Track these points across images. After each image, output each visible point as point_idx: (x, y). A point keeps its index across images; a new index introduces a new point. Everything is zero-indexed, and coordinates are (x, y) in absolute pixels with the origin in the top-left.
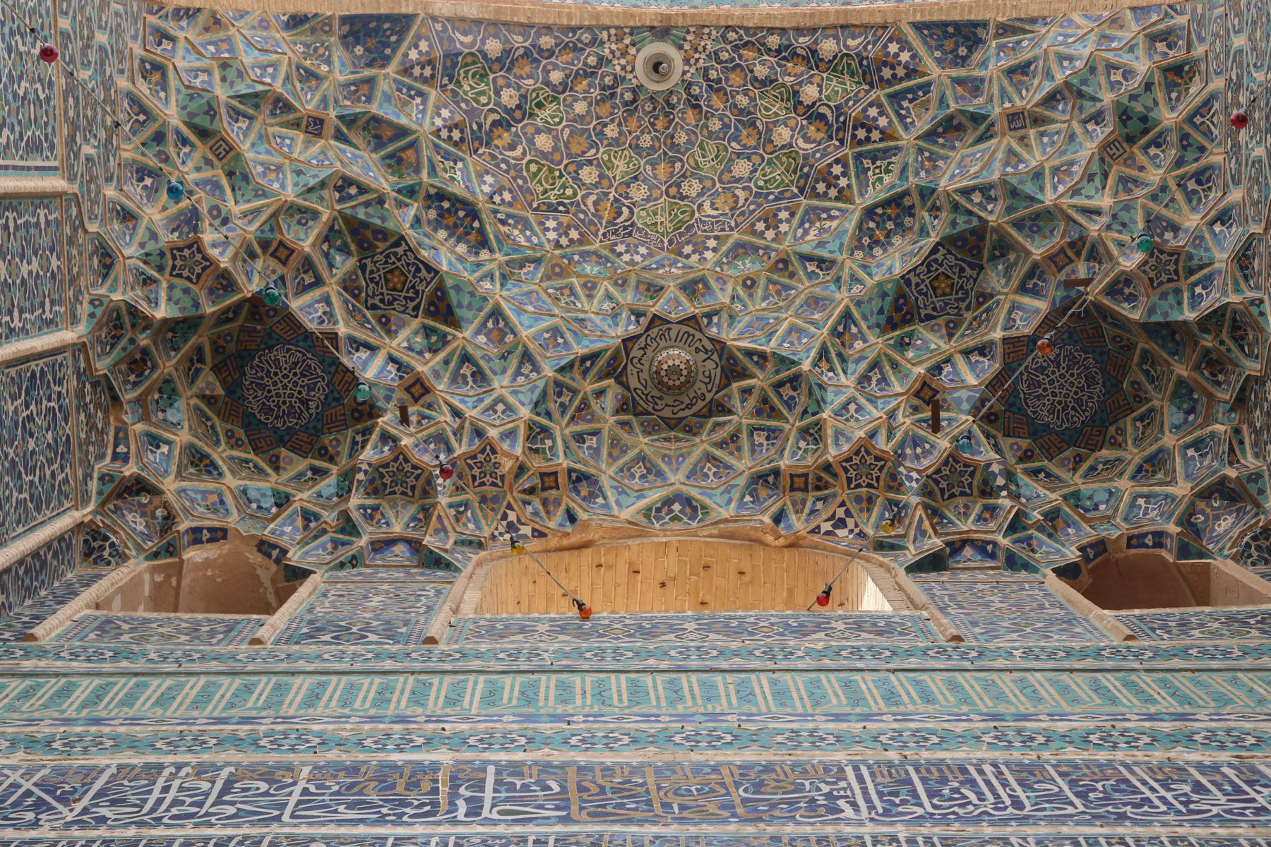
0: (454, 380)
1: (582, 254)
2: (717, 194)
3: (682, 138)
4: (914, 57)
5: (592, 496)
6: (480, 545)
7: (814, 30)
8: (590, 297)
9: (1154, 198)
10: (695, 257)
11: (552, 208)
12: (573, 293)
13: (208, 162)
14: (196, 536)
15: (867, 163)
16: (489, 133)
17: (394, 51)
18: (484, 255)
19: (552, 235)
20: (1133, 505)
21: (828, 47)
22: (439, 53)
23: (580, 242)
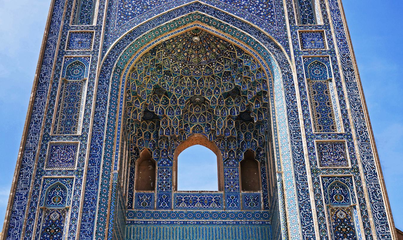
0: (169, 110)
1: (185, 68)
2: (204, 57)
3: (199, 47)
4: (234, 49)
5: (187, 126)
6: (174, 150)
7: (219, 38)
8: (186, 80)
9: (259, 109)
10: (201, 69)
11: (180, 61)
12: (184, 80)
13: (136, 98)
14: (141, 151)
15: (226, 59)
16: (171, 52)
17: (157, 48)
18: (171, 77)
19: (180, 67)
20: (252, 141)
21: (221, 41)
22: (163, 45)
23: (185, 66)
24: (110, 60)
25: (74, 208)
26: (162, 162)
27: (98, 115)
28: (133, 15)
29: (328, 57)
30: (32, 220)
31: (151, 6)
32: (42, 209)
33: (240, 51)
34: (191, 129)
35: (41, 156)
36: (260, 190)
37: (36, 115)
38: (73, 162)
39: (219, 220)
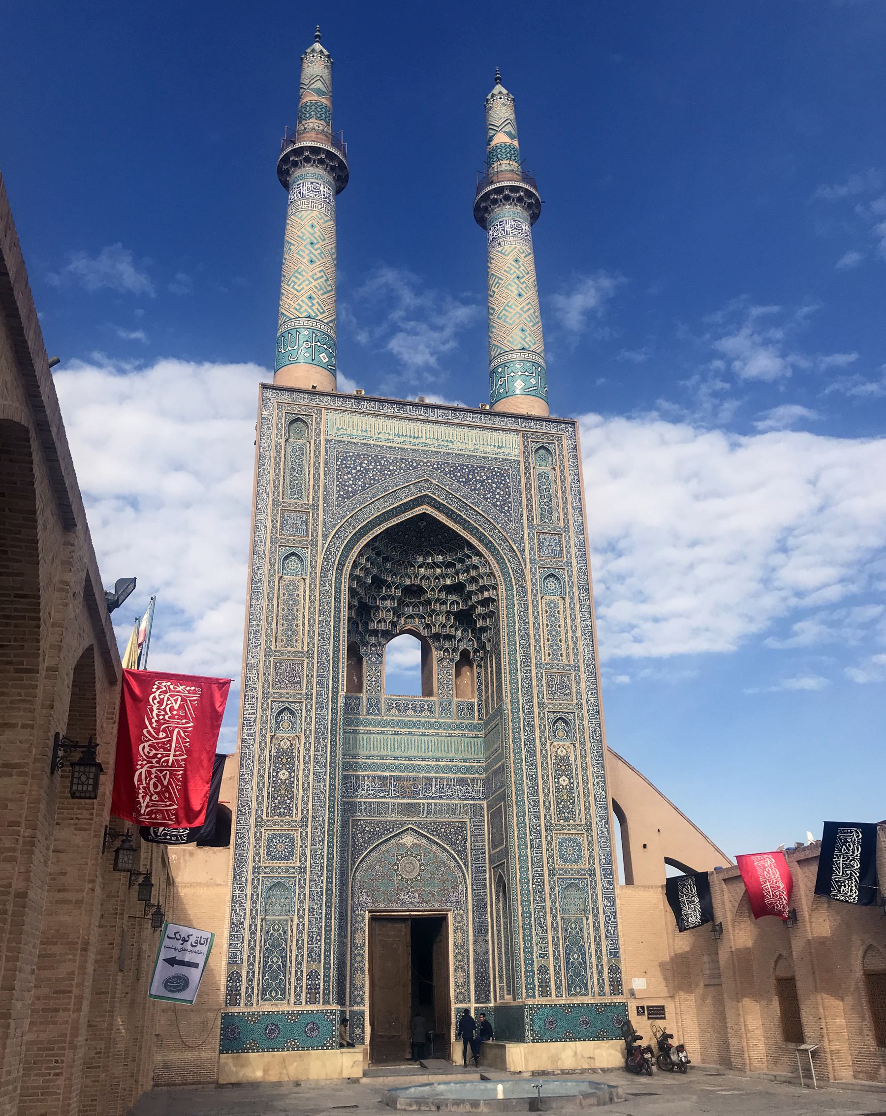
24: (331, 554)
25: (306, 737)
26: (370, 659)
27: (322, 626)
28: (354, 492)
29: (564, 569)
30: (262, 749)
31: (374, 479)
32: (272, 737)
33: (471, 546)
34: (403, 619)
35: (265, 674)
36: (473, 697)
37: (255, 623)
38: (300, 682)
39: (432, 730)
